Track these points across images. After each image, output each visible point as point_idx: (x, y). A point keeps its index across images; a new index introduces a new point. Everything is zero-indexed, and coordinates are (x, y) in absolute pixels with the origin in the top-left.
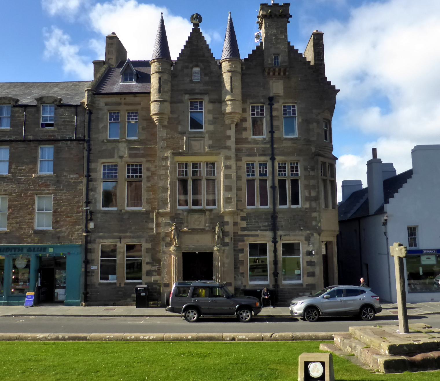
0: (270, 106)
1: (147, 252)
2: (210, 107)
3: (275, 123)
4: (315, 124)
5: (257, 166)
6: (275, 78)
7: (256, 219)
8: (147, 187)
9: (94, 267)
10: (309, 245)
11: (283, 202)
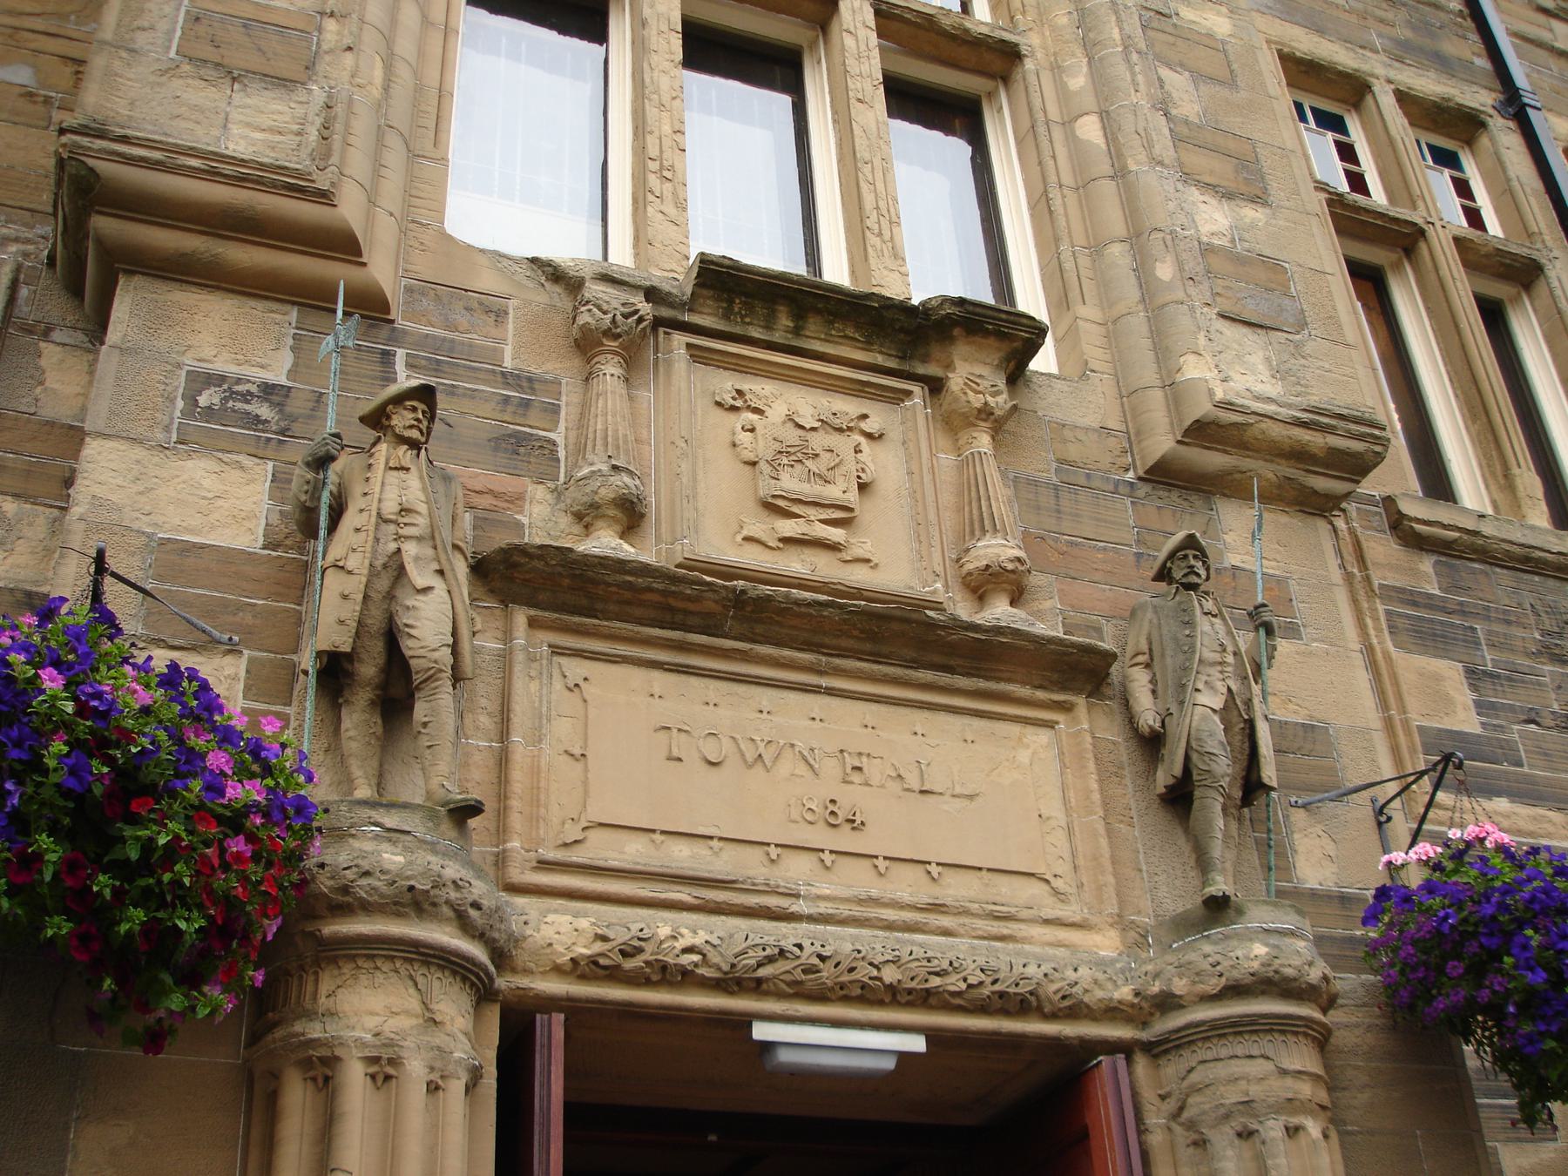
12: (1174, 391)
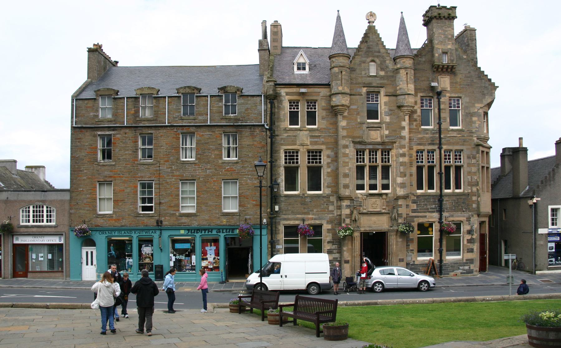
1: (328, 232)
5: (425, 154)
7: (424, 202)
11: (448, 187)
12: (396, 194)
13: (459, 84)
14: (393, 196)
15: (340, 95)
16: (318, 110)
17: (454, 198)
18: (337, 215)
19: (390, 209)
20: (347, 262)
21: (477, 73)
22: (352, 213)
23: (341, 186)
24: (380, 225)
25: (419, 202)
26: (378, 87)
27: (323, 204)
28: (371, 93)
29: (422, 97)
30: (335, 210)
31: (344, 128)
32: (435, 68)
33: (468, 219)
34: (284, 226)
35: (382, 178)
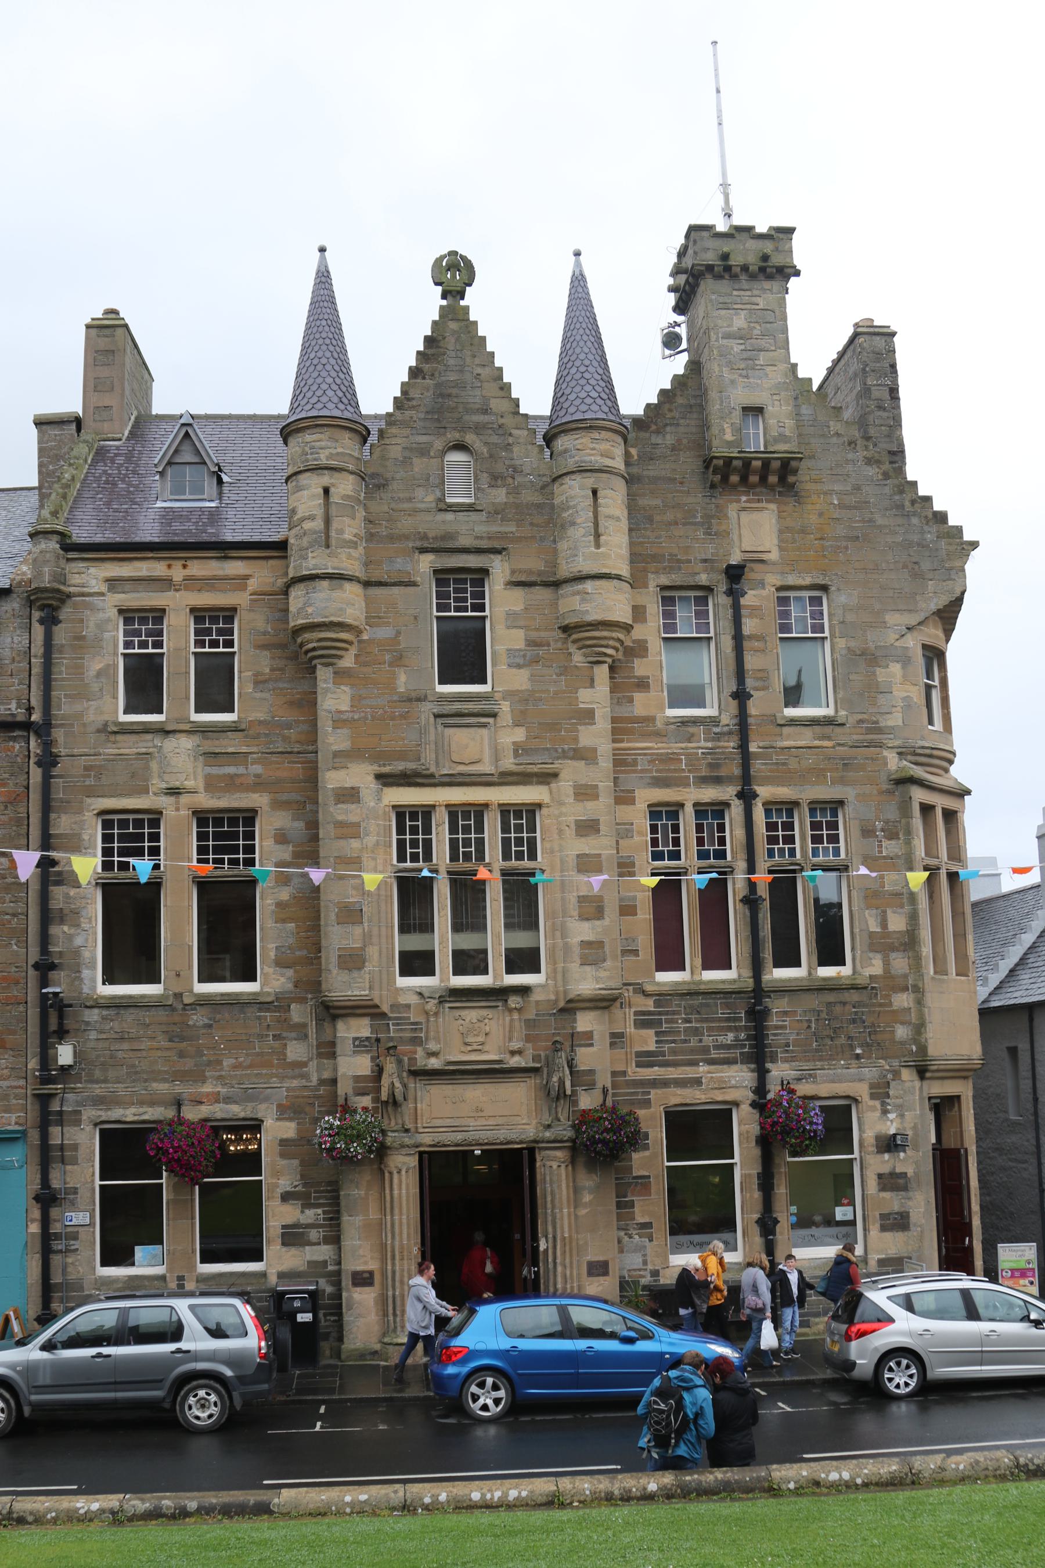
0: (730, 599)
1: (283, 1155)
2: (515, 600)
3: (751, 662)
4: (896, 668)
5: (688, 820)
6: (747, 493)
7: (690, 1022)
8: (280, 905)
9: (78, 1218)
10: (885, 1112)
12: (565, 992)
13: (818, 536)
14: (553, 997)
15: (325, 583)
16: (240, 649)
17: (814, 1002)
18: (322, 1082)
19: (543, 1054)
20: (363, 1279)
21: (887, 490)
22: (379, 1072)
23: (330, 958)
24: (500, 1121)
25: (667, 1021)
26: (479, 551)
27: (261, 1037)
28: (451, 577)
29: (664, 588)
30: (311, 1059)
31: (339, 722)
32: (715, 473)
33: (881, 1092)
34: (103, 1132)
35: (508, 926)
